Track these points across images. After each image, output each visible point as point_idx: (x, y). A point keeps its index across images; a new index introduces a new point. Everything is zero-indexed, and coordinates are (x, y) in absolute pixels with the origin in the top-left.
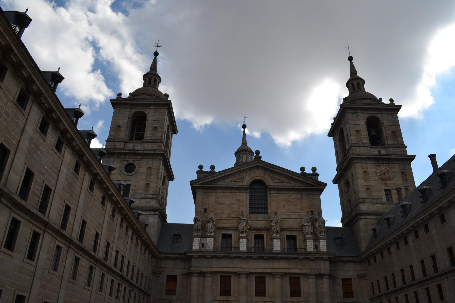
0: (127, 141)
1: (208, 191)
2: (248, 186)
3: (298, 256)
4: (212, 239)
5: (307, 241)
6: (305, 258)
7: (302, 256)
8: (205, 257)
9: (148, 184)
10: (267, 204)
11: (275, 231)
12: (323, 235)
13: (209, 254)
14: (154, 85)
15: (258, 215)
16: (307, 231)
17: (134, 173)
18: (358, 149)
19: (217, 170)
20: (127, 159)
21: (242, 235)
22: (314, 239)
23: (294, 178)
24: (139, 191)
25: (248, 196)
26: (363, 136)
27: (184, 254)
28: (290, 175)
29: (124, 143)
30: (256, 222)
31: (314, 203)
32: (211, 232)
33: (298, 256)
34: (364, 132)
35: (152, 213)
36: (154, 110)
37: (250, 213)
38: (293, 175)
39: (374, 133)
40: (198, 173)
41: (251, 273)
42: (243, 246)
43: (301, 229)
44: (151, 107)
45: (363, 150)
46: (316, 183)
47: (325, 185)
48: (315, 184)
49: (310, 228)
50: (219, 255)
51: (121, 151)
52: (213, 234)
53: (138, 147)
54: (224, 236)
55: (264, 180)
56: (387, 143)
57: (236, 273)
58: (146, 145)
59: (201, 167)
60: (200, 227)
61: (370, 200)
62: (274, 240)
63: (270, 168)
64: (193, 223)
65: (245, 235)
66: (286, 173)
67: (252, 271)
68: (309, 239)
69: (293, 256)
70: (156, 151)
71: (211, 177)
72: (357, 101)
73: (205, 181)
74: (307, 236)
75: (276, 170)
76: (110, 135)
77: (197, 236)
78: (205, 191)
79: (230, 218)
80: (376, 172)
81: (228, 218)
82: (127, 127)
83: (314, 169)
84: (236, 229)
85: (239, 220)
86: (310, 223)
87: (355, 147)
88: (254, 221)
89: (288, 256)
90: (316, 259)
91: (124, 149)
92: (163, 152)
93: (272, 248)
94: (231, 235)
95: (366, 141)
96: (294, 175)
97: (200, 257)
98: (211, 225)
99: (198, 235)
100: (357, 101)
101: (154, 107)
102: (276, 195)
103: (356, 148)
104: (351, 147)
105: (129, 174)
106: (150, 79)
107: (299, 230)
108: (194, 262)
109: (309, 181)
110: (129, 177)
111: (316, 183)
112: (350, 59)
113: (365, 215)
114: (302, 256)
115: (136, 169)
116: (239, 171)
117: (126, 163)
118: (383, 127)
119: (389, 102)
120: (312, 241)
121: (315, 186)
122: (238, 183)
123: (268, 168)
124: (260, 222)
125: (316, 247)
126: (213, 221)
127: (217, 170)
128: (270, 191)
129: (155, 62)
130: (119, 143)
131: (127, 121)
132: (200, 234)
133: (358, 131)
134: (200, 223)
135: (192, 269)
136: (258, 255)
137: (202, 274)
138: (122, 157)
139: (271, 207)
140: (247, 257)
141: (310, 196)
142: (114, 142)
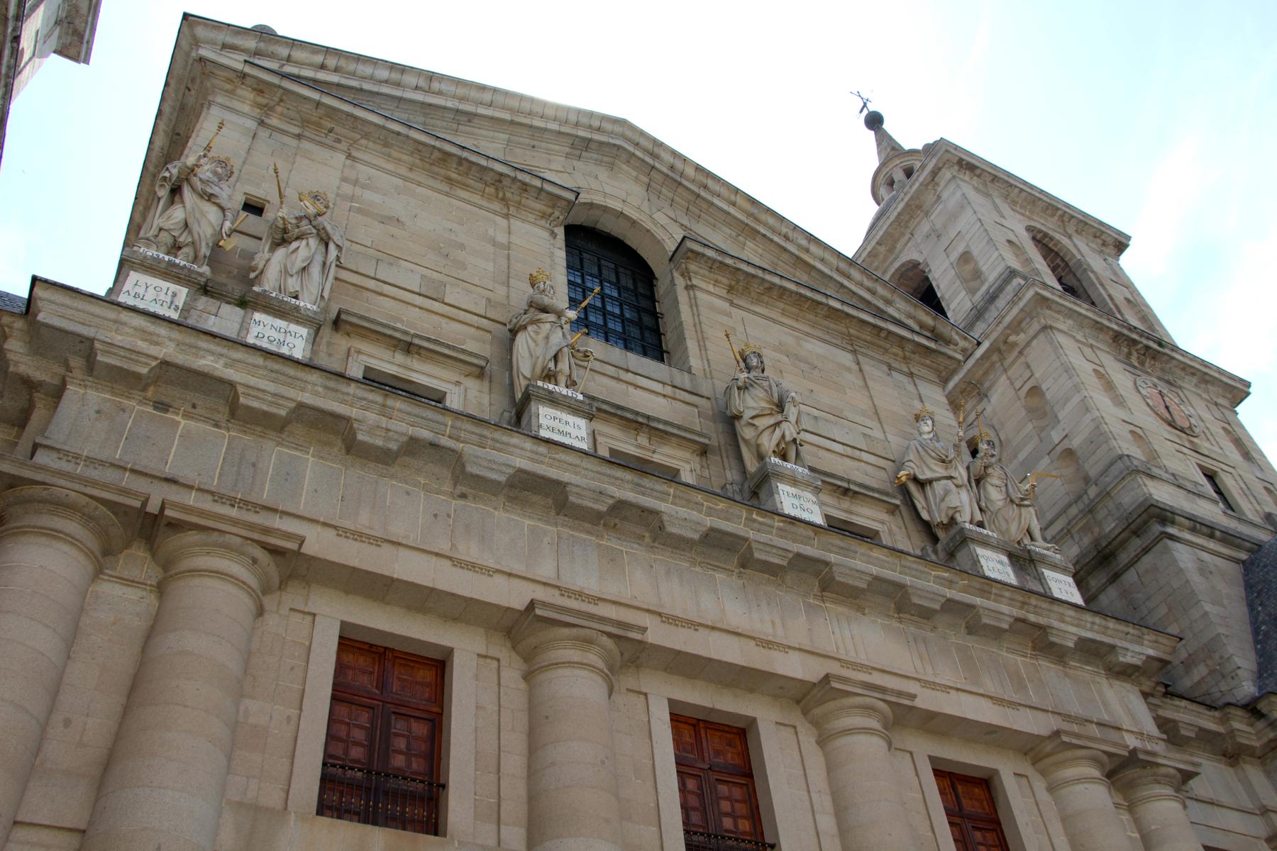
3: (978, 601)
30: (624, 386)
33: (978, 601)
38: (807, 251)
50: (372, 417)
69: (950, 593)
71: (336, 70)
73: (289, 69)
75: (716, 201)
89: (920, 583)
99: (171, 264)
102: (726, 305)
112: (874, 121)
114: (1005, 609)
116: (512, 122)
128: (686, 274)
139: (702, 347)
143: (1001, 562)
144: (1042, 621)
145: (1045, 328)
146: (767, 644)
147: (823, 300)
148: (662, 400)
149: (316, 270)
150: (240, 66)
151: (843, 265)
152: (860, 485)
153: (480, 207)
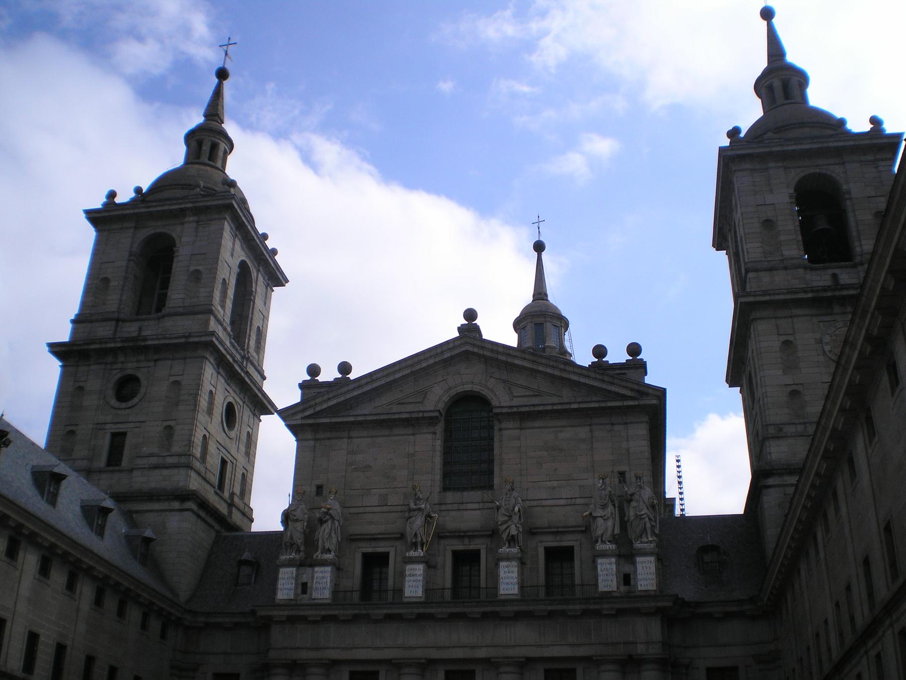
0: (122, 316)
1: (328, 435)
2: (437, 414)
4: (329, 569)
5: (600, 561)
6: (585, 613)
7: (577, 607)
8: (304, 619)
9: (169, 428)
10: (491, 462)
11: (505, 536)
12: (647, 543)
13: (314, 612)
14: (209, 159)
15: (465, 493)
16: (599, 532)
17: (135, 400)
18: (765, 278)
19: (352, 376)
20: (119, 366)
21: (412, 553)
22: (619, 556)
23: (569, 380)
24: (145, 450)
25: (439, 443)
26: (782, 238)
27: (253, 613)
28: (557, 373)
29: (114, 322)
31: (628, 450)
32: (329, 551)
34: (789, 224)
35: (176, 505)
36: (194, 225)
37: (445, 489)
39: (822, 224)
40: (303, 386)
41: (432, 662)
42: (414, 584)
43: (586, 529)
44: (187, 219)
45: (780, 280)
46: (632, 390)
47: (661, 394)
48: (629, 393)
49: (610, 523)
50: (341, 612)
51: (103, 346)
52: (330, 556)
53: (151, 330)
54: (458, 557)
55: (485, 392)
56: (858, 249)
57: (388, 662)
58: (168, 323)
59: (314, 370)
60: (299, 539)
61: (800, 428)
62: (502, 564)
63: (500, 357)
64: (281, 528)
65: (420, 553)
66: (547, 365)
67: (435, 654)
68: (604, 554)
69: (550, 608)
70: (190, 336)
71: (334, 397)
72: (770, 135)
73: (318, 409)
74: (600, 547)
75: (517, 362)
76: (84, 304)
77: (290, 564)
78: (321, 435)
79: (385, 509)
80: (820, 341)
81: (378, 509)
82: (126, 278)
83: (634, 349)
84: (402, 536)
85: (409, 513)
86: (610, 508)
87: (756, 270)
88: (453, 513)
90: (621, 612)
91: (113, 339)
92: (208, 339)
93: (496, 588)
94: (386, 556)
95: (794, 251)
96: (569, 372)
97: (292, 620)
98: (327, 531)
100: (770, 135)
101: (195, 218)
102: (517, 432)
103: (761, 274)
104: (747, 271)
105: (124, 405)
106: (200, 144)
107: (582, 532)
108: (279, 637)
109: (612, 384)
110: (123, 412)
111: (632, 390)
112: (767, 14)
113: (781, 475)
114: (577, 607)
115: (142, 390)
117: (116, 376)
118: (848, 203)
119: (867, 127)
120: (613, 560)
121: (631, 398)
122: (409, 408)
123: (495, 356)
124: (468, 513)
125: (627, 579)
126: (332, 517)
127: (352, 376)
129: (218, 94)
130: (104, 324)
131: (124, 263)
132: (297, 557)
133: (768, 224)
134: (299, 526)
135: (272, 654)
136: (449, 610)
137: (294, 667)
138: (110, 359)
140: (421, 617)
141: (616, 428)
142: (91, 322)
143: (611, 564)
144: (597, 607)
145: (752, 320)
146: (473, 647)
147: (568, 407)
148: (478, 512)
149: (333, 535)
150: (299, 422)
151: (584, 372)
152: (564, 527)
153: (403, 435)
